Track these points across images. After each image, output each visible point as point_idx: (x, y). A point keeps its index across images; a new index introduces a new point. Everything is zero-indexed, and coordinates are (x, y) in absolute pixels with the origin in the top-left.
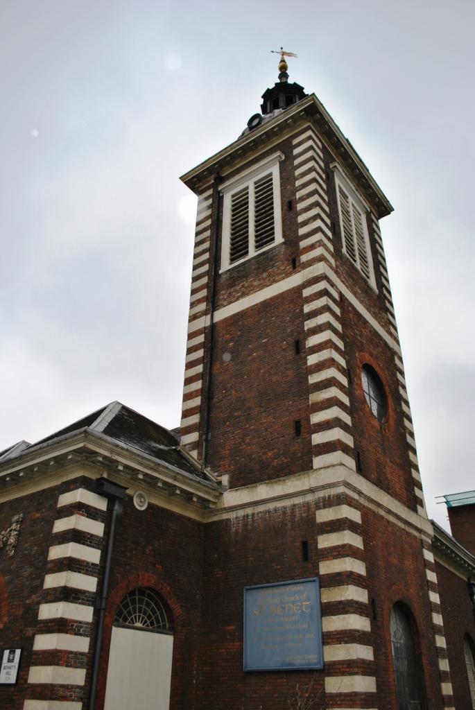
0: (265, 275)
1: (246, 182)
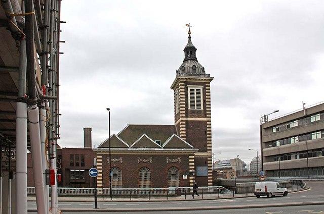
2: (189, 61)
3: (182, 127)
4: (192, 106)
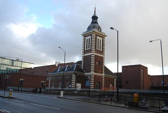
3: (93, 58)
4: (98, 48)
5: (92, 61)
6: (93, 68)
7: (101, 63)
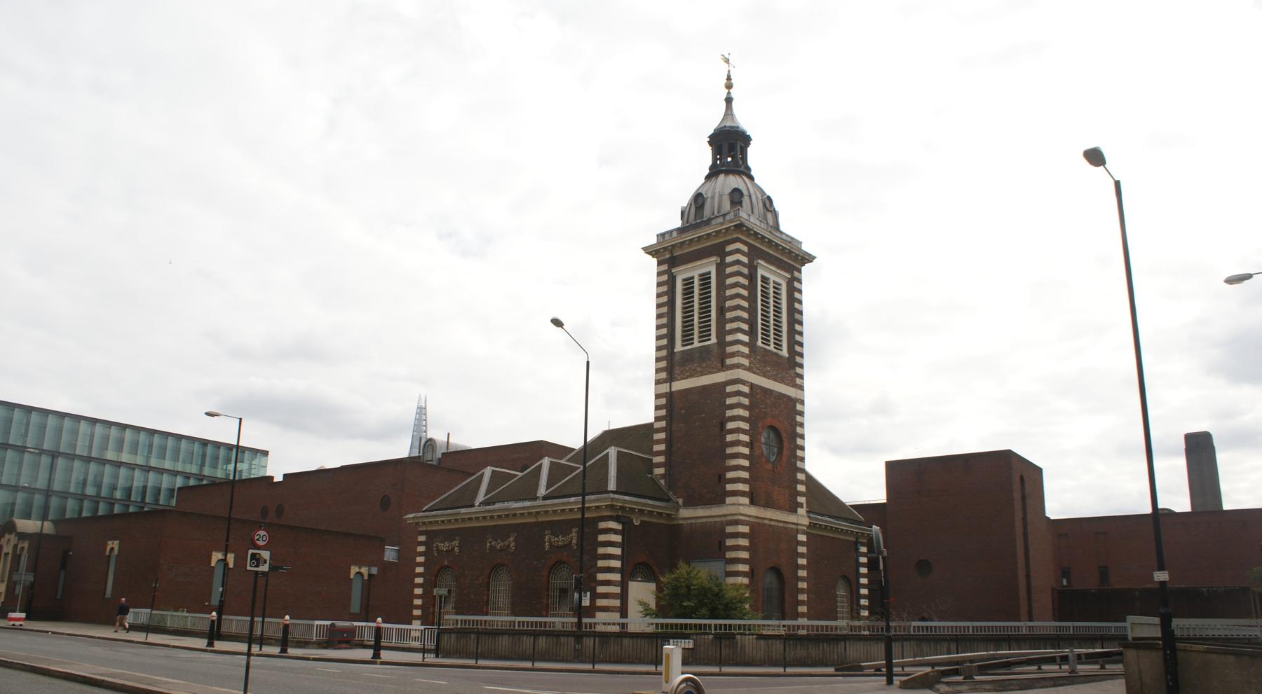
0: (704, 365)
1: (693, 271)
2: (722, 177)
5: (730, 425)
6: (738, 475)
7: (786, 444)
